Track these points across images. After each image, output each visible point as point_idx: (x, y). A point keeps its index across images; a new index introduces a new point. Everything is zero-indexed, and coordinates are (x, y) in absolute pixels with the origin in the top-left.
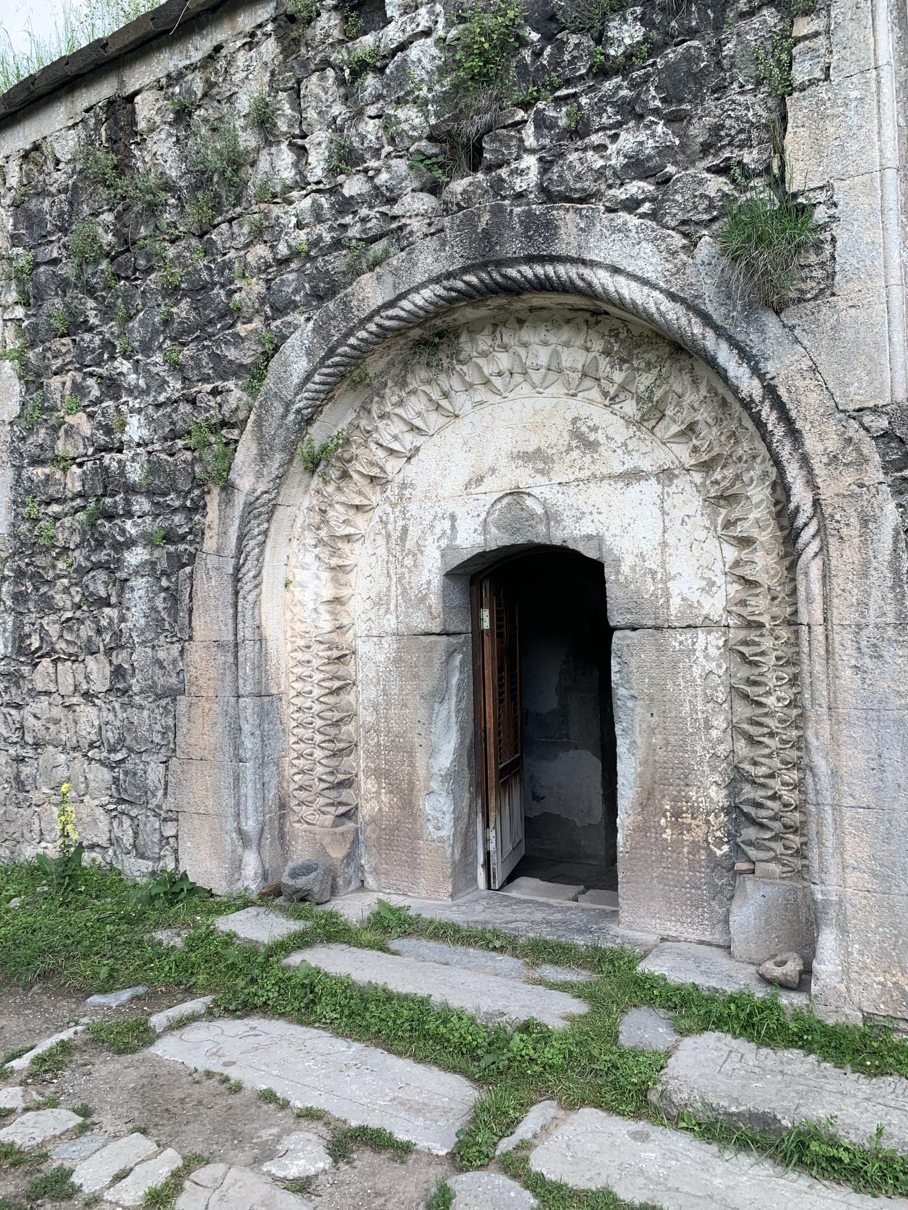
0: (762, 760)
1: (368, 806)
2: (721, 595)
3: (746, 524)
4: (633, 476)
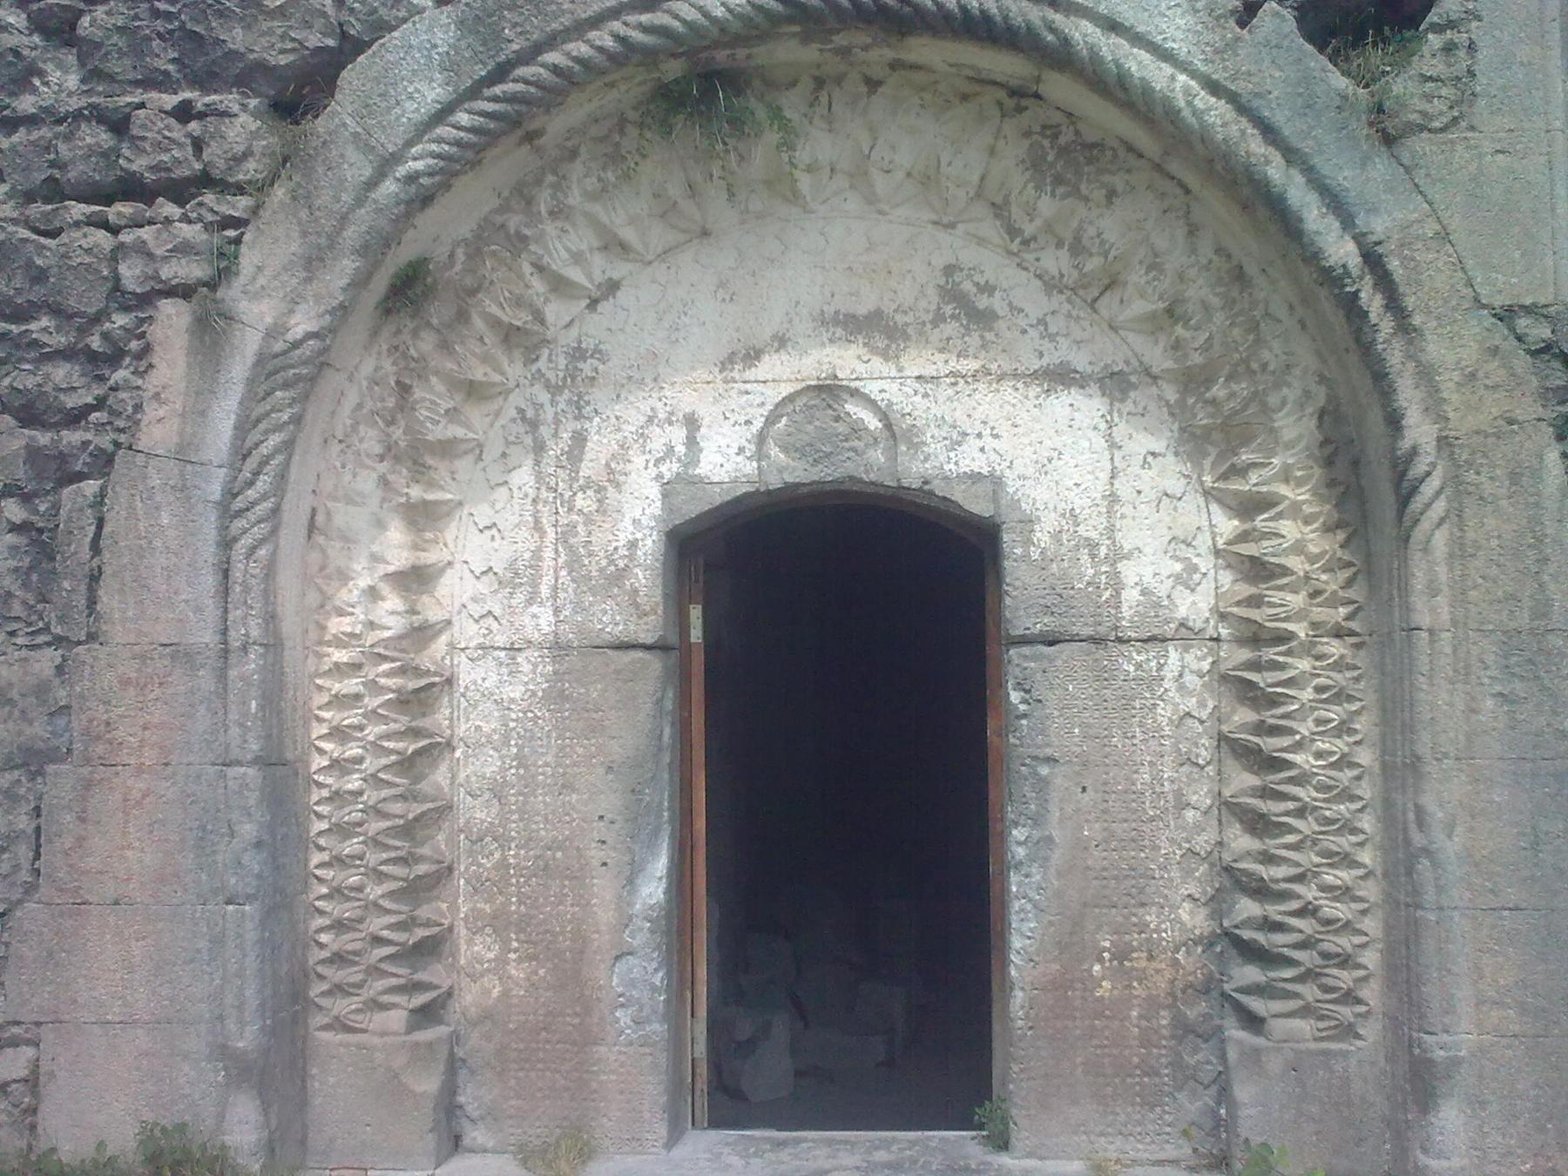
0: (1284, 853)
1: (475, 988)
2: (1207, 587)
3: (1266, 472)
4: (1059, 377)
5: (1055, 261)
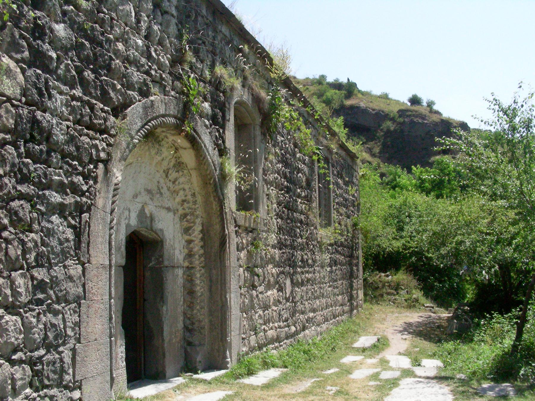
4: (169, 209)
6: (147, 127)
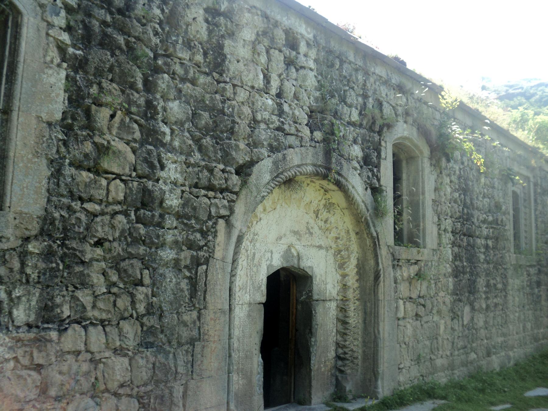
4: (320, 247)
5: (322, 224)
6: (278, 179)
